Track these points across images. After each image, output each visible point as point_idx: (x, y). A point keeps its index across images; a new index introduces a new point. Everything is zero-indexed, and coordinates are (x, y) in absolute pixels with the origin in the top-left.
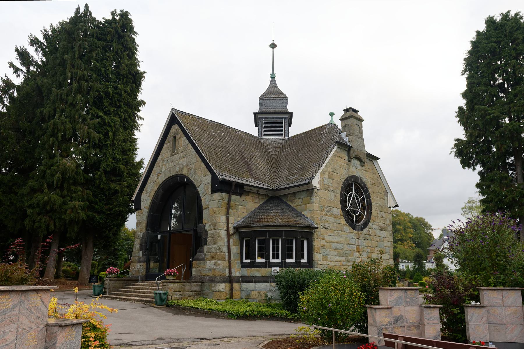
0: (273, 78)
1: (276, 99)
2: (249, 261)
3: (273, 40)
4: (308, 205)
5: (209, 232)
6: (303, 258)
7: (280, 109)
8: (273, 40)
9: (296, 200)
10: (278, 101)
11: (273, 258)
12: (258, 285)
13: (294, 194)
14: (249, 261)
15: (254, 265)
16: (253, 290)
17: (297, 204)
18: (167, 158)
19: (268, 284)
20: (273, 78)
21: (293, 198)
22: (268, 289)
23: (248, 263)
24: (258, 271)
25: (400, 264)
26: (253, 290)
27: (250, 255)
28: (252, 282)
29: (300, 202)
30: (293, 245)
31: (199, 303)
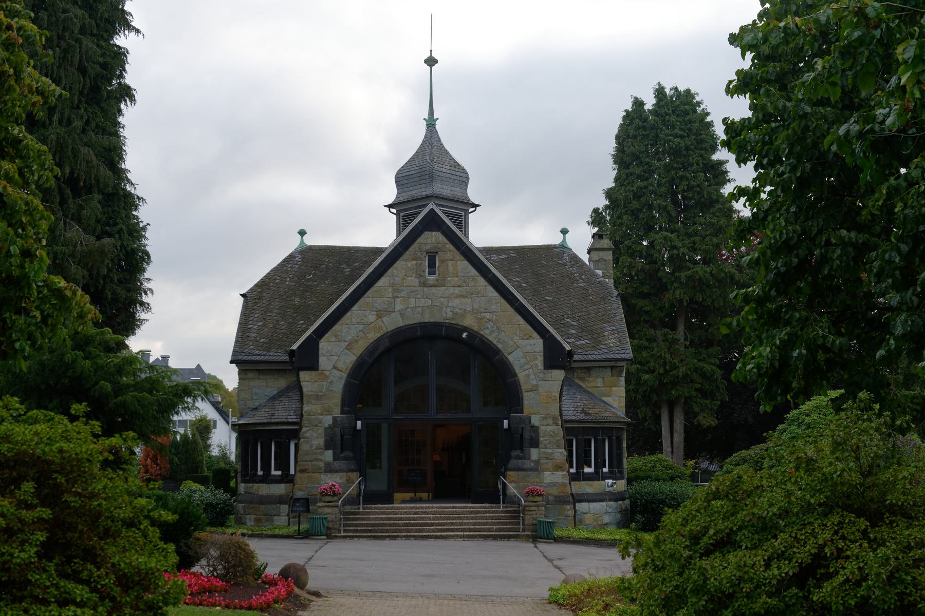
0: (431, 124)
1: (453, 172)
2: (279, 473)
3: (431, 51)
4: (614, 388)
5: (543, 428)
6: (605, 467)
7: (456, 192)
8: (431, 51)
9: (591, 379)
10: (455, 177)
11: (275, 470)
12: (594, 506)
13: (588, 369)
14: (279, 473)
15: (579, 476)
16: (587, 513)
17: (593, 384)
18: (406, 286)
19: (604, 504)
20: (431, 124)
21: (585, 375)
22: (605, 511)
23: (279, 476)
24: (591, 486)
25: (509, 473)
26: (587, 513)
27: (584, 460)
28: (584, 501)
29: (599, 382)
30: (591, 447)
31: (576, 534)
